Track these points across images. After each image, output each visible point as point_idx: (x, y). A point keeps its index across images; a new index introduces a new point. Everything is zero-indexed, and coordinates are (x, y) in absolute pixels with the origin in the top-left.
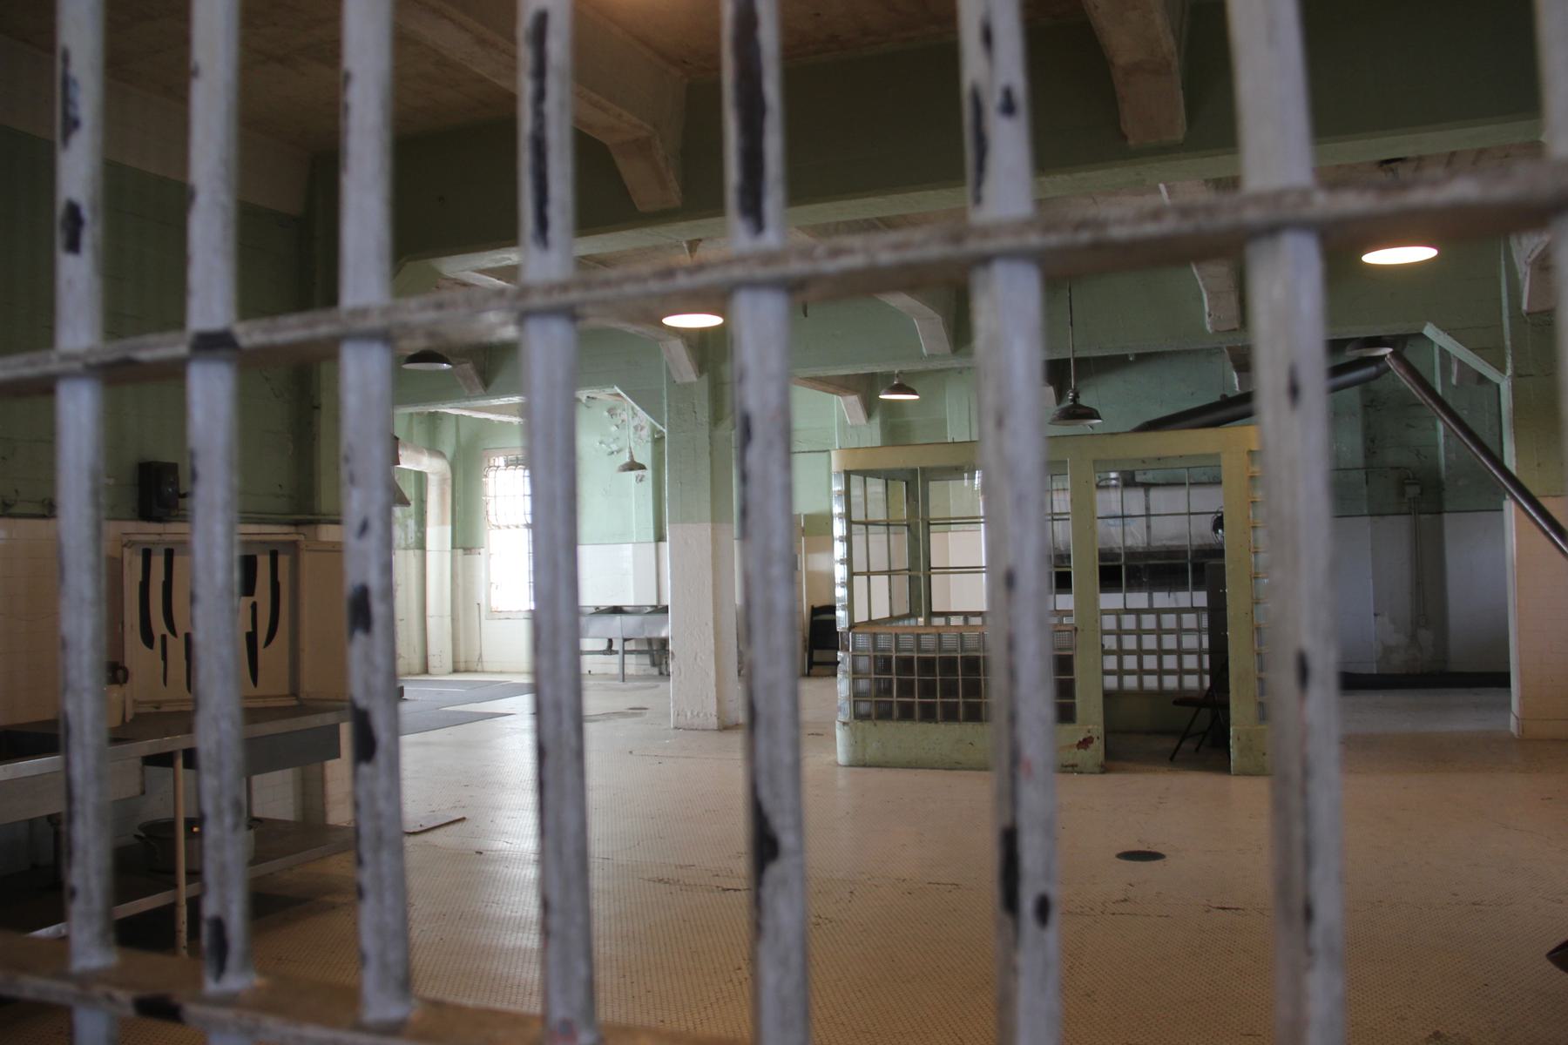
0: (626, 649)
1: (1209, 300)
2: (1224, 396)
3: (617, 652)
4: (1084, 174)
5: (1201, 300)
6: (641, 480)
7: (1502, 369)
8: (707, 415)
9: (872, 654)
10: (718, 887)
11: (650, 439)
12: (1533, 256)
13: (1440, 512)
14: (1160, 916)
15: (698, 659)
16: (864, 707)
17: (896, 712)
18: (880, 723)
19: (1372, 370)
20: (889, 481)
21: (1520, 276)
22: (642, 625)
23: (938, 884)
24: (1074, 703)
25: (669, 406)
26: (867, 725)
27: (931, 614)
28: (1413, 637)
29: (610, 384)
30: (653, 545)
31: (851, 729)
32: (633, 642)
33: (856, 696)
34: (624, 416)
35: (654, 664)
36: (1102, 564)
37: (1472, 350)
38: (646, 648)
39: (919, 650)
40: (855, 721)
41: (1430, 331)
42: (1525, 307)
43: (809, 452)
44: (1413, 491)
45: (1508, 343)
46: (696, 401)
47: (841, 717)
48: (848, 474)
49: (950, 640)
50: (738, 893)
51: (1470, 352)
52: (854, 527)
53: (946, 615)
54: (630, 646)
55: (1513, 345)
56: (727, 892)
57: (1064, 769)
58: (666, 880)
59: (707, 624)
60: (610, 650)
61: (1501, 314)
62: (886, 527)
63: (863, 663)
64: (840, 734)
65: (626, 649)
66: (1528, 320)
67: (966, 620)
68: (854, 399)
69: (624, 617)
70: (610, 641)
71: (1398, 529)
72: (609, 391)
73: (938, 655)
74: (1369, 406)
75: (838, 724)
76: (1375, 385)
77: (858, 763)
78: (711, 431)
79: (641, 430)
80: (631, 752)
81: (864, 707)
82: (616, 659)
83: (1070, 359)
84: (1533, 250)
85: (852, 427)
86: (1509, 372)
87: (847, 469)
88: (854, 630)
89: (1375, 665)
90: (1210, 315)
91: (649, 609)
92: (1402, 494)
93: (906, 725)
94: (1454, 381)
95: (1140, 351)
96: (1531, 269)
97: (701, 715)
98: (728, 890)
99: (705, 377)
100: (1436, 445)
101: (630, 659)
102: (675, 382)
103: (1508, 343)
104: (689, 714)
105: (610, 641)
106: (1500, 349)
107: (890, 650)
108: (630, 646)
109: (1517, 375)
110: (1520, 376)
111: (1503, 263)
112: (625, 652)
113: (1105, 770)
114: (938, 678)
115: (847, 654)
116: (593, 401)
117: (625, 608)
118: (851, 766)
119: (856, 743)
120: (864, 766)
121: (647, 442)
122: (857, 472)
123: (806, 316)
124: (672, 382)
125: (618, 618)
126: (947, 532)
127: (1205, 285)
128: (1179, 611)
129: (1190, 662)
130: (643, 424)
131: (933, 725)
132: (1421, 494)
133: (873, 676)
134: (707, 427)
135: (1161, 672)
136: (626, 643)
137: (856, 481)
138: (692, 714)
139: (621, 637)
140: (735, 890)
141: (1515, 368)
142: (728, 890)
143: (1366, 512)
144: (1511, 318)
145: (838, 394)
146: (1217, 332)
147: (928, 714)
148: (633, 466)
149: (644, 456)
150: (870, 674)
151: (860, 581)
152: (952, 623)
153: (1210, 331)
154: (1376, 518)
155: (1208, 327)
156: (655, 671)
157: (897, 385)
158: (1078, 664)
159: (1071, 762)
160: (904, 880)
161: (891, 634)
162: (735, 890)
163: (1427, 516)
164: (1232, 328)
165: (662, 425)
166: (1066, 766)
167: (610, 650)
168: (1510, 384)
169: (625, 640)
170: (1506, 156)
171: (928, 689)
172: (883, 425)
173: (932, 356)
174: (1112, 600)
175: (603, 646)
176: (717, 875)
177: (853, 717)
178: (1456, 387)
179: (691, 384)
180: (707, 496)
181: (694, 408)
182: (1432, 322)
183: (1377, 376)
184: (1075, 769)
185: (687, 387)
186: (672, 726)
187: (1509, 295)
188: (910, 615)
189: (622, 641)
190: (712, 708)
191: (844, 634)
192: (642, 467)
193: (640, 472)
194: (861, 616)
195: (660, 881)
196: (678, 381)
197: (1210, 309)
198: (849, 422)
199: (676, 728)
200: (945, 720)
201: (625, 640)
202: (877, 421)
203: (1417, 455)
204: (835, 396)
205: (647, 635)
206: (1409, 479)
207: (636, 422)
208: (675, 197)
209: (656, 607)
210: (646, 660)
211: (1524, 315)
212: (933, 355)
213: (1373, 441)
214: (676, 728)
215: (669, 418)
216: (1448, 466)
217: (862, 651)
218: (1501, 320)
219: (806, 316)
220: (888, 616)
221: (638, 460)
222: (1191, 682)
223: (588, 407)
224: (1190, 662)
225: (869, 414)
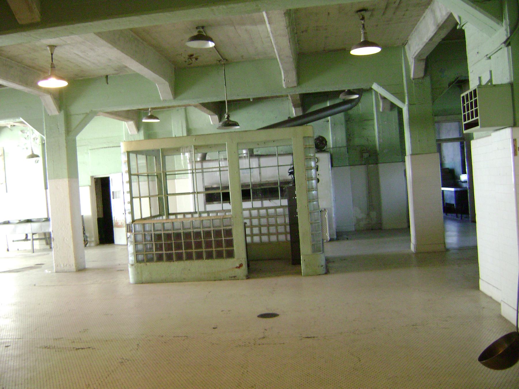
0: (34, 238)
1: (284, 73)
2: (289, 118)
3: (30, 240)
4: (232, 5)
5: (281, 74)
6: (37, 162)
7: (404, 102)
8: (64, 129)
9: (143, 233)
10: (74, 348)
11: (41, 144)
12: (415, 55)
13: (377, 164)
14: (280, 344)
15: (65, 241)
16: (141, 257)
17: (155, 258)
18: (148, 264)
19: (349, 106)
20: (148, 157)
21: (410, 64)
22: (41, 227)
23: (178, 337)
24: (233, 250)
25: (46, 126)
26: (142, 264)
27: (169, 214)
28: (368, 215)
29: (18, 116)
30: (45, 190)
31: (135, 267)
32: (37, 235)
33: (137, 252)
34: (28, 133)
35: (47, 244)
36: (243, 189)
37: (392, 94)
38: (43, 237)
39: (164, 230)
40: (137, 263)
41: (375, 86)
42: (412, 76)
43: (113, 147)
44: (366, 155)
45: (406, 91)
46: (59, 124)
47: (131, 262)
48: (128, 153)
49: (177, 225)
50: (83, 350)
52: (133, 177)
53: (175, 214)
54: (35, 237)
55: (408, 93)
56: (78, 350)
57: (230, 278)
58: (48, 347)
59: (68, 224)
60: (26, 239)
61: (403, 79)
62: (147, 177)
63: (140, 237)
64: (130, 270)
65: (34, 238)
66: (413, 82)
67: (184, 216)
68: (131, 123)
69: (33, 224)
70: (27, 235)
71: (361, 171)
72: (17, 120)
73: (172, 232)
74: (348, 121)
75: (129, 265)
76: (350, 112)
77: (140, 282)
78: (66, 137)
79: (36, 140)
80: (35, 285)
81: (141, 257)
82: (29, 243)
83: (225, 101)
84: (415, 52)
85: (131, 135)
86: (407, 103)
87: (128, 151)
88: (134, 223)
89: (354, 226)
90: (284, 80)
91: (44, 220)
92: (362, 156)
93: (160, 264)
94: (381, 110)
95: (255, 97)
96: (414, 60)
97: (68, 265)
98: (79, 349)
99: (62, 112)
100: (375, 137)
101: (36, 243)
102: (48, 115)
103: (406, 91)
104: (62, 265)
105: (27, 235)
106: (403, 93)
107: (151, 231)
108: (35, 237)
109: (410, 104)
111: (403, 58)
112: (33, 240)
113: (248, 277)
114: (173, 242)
115: (132, 233)
116: (14, 127)
117: (33, 220)
118: (136, 283)
119: (138, 273)
120: (142, 283)
121: (39, 145)
122: (133, 152)
123: (108, 84)
124: (47, 115)
125: (29, 224)
126: (175, 179)
127: (283, 68)
128: (275, 208)
129: (281, 229)
130: (37, 137)
131: (172, 263)
132: (370, 156)
133: (144, 243)
134: (64, 135)
135: (269, 234)
136: (34, 235)
137: (132, 156)
138: (64, 265)
139: (31, 233)
140: (82, 349)
141: (409, 101)
142: (79, 349)
143: (348, 165)
144: (407, 80)
145: (124, 121)
146: (288, 88)
147: (170, 258)
148: (33, 156)
149: (38, 151)
150: (143, 242)
151: (136, 201)
152: (178, 217)
153: (285, 87)
154: (352, 167)
155: (284, 86)
156: (48, 247)
157: (150, 115)
158: (234, 233)
159: (233, 275)
160: (162, 336)
161: (151, 223)
162: (82, 349)
163: (372, 165)
164: (294, 86)
165: (43, 135)
166: (231, 277)
167: (26, 239)
168: (407, 108)
169: (33, 234)
170: (407, 10)
171: (169, 247)
172: (145, 133)
173: (165, 101)
174: (247, 205)
175: (24, 237)
176: (74, 342)
177: (136, 261)
178: (382, 112)
179: (56, 116)
180: (65, 166)
181: (58, 126)
182: (375, 82)
183: (350, 108)
184: (236, 278)
185: (54, 117)
186: (55, 271)
187: (406, 71)
188: (160, 215)
189: (32, 234)
190: (73, 261)
191: (130, 225)
192: (37, 156)
193: (37, 158)
194: (137, 216)
195: (45, 347)
196: (50, 114)
197: (285, 78)
198: (130, 133)
199: (56, 272)
200: (178, 260)
201: (33, 234)
202: (142, 132)
203: (367, 141)
204: (123, 122)
205: (43, 231)
206: (365, 150)
207: (34, 136)
208: (37, 17)
209: (47, 218)
210: (44, 242)
211: (412, 80)
212: (165, 100)
213: (349, 135)
214: (56, 272)
215: (46, 132)
216: (379, 145)
217: (139, 232)
218: (403, 82)
219: (108, 84)
220: (150, 216)
221: (35, 153)
222: (282, 238)
223: (12, 130)
224: (281, 229)
225: (138, 129)
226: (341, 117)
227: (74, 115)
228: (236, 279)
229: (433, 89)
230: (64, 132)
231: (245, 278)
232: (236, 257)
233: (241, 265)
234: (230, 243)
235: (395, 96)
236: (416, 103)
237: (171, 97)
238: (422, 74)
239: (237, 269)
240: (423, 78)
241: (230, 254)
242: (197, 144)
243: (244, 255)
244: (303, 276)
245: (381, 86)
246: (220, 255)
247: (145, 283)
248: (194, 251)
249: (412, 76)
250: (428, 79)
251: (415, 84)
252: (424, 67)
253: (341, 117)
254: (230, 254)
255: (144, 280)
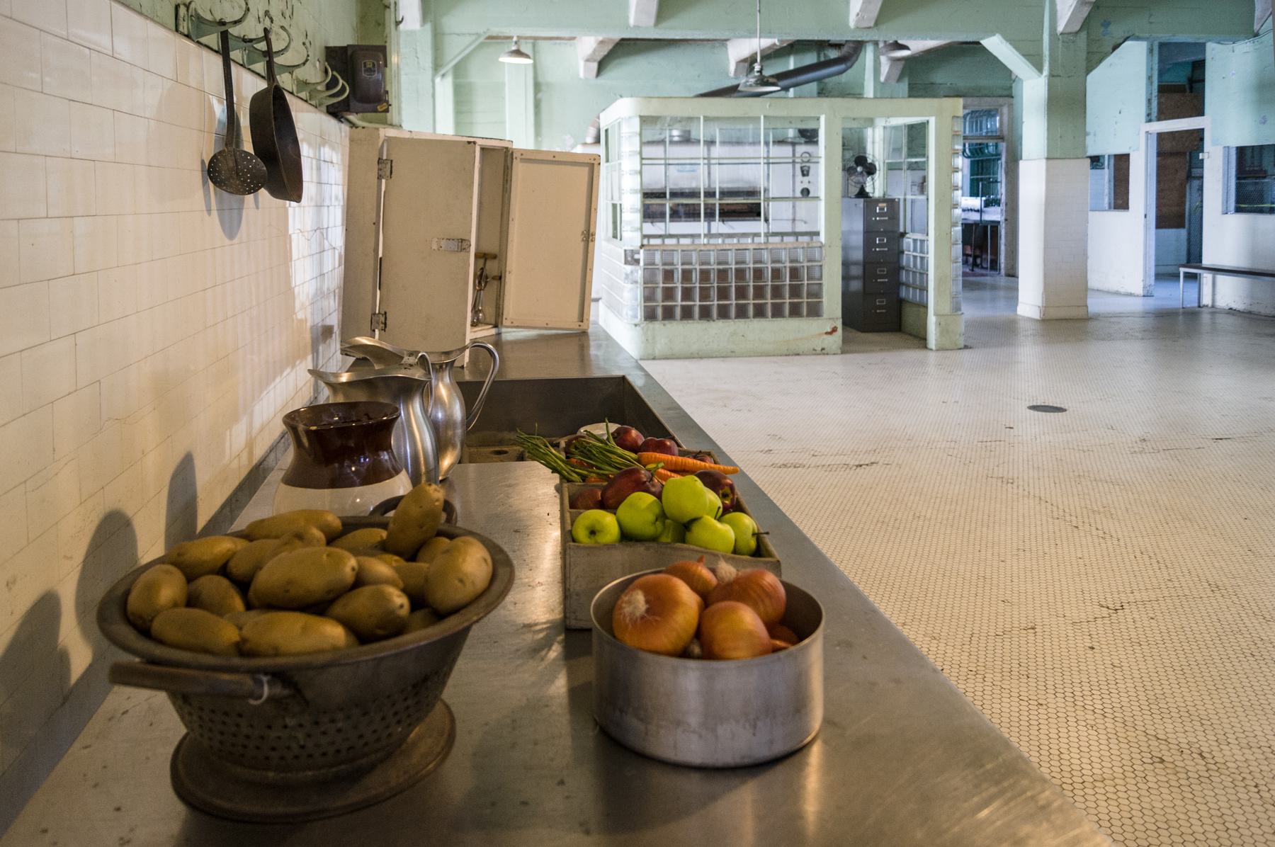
7: (1040, 70)
24: (821, 302)
37: (1024, 55)
42: (1060, 28)
45: (1046, 52)
46: (418, 49)
51: (1022, 57)
55: (1051, 56)
94: (882, 79)
99: (428, 27)
103: (1046, 52)
109: (1052, 76)
110: (1053, 76)
113: (842, 353)
131: (712, 323)
178: (883, 83)
181: (416, 53)
218: (1042, 37)
226: (813, 87)
227: (450, 34)
228: (824, 354)
229: (1088, 53)
230: (431, 65)
231: (839, 351)
232: (825, 316)
233: (834, 330)
234: (816, 293)
235: (1028, 60)
236: (1061, 74)
237: (652, 21)
238: (1077, 28)
239: (825, 336)
240: (1077, 33)
241: (815, 311)
242: (771, 113)
243: (839, 313)
244: (940, 349)
245: (1007, 40)
246: (795, 312)
247: (660, 359)
248: (769, 301)
249: (1060, 28)
250: (1083, 35)
251: (1063, 42)
252: (1085, 15)
253: (813, 87)
254: (815, 311)
255: (657, 353)
